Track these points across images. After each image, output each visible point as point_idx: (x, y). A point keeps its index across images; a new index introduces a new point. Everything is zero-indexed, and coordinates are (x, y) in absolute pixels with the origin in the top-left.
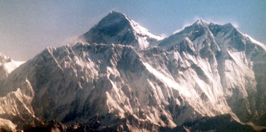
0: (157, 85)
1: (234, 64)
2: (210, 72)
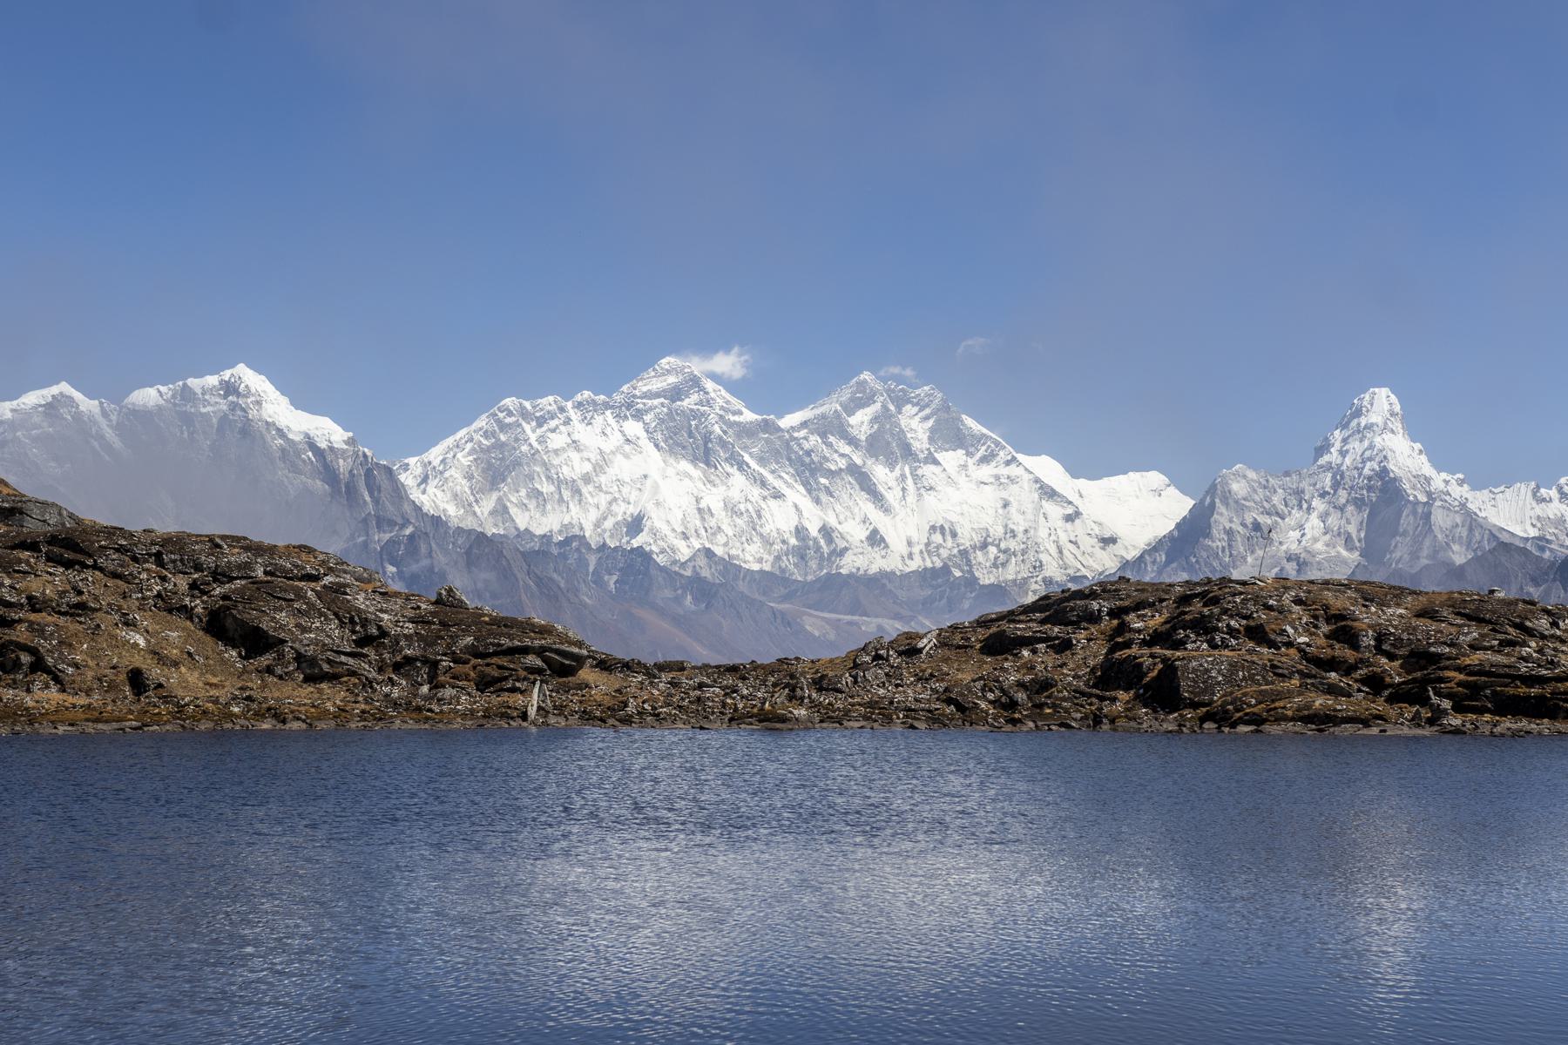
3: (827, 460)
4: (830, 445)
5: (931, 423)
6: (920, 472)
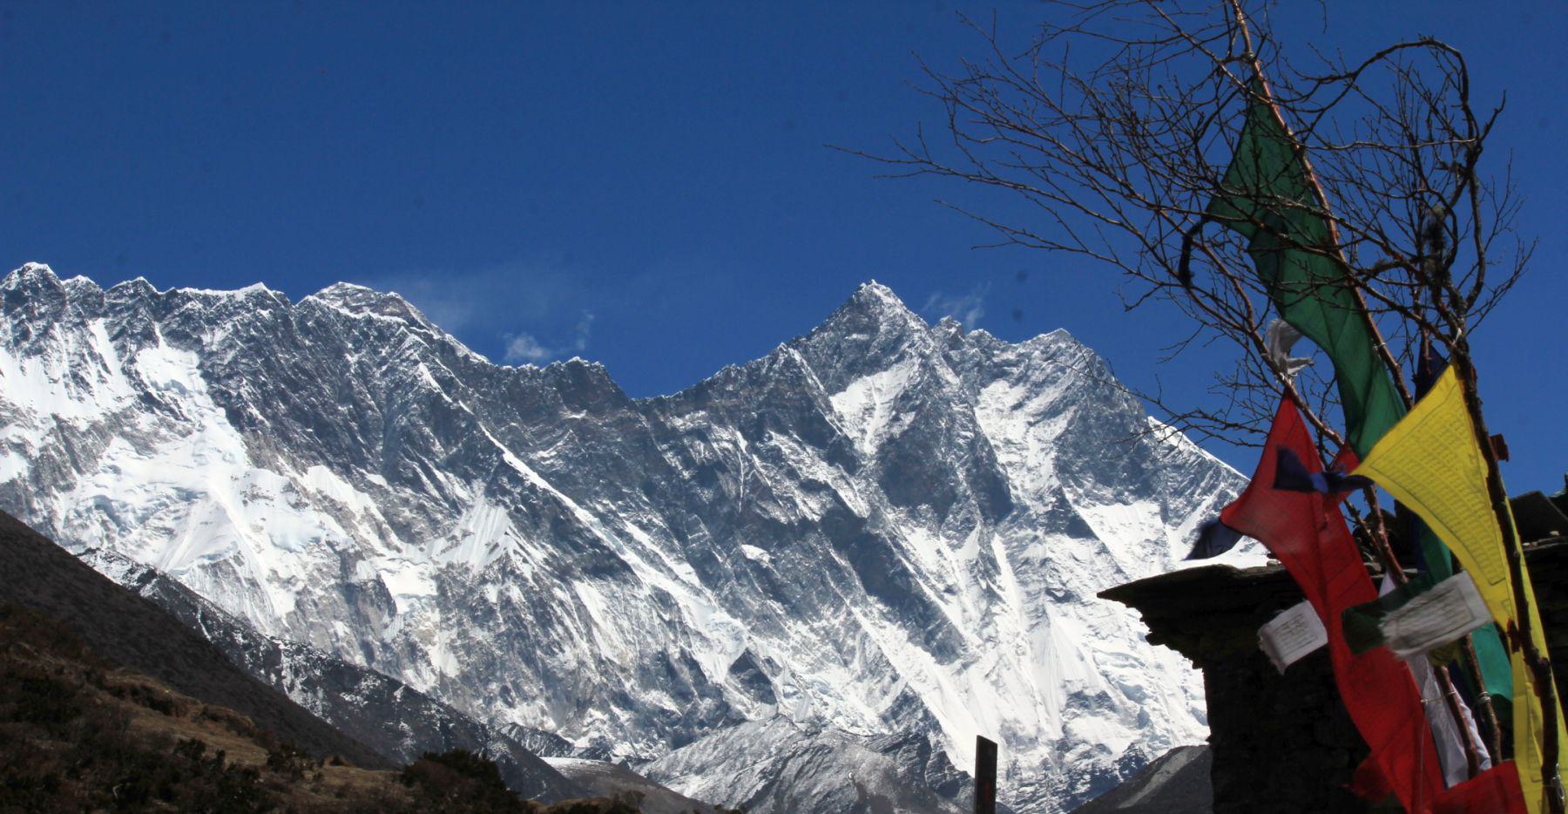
0: (578, 571)
2: (949, 590)
3: (765, 493)
4: (775, 457)
5: (1060, 425)
6: (1035, 552)
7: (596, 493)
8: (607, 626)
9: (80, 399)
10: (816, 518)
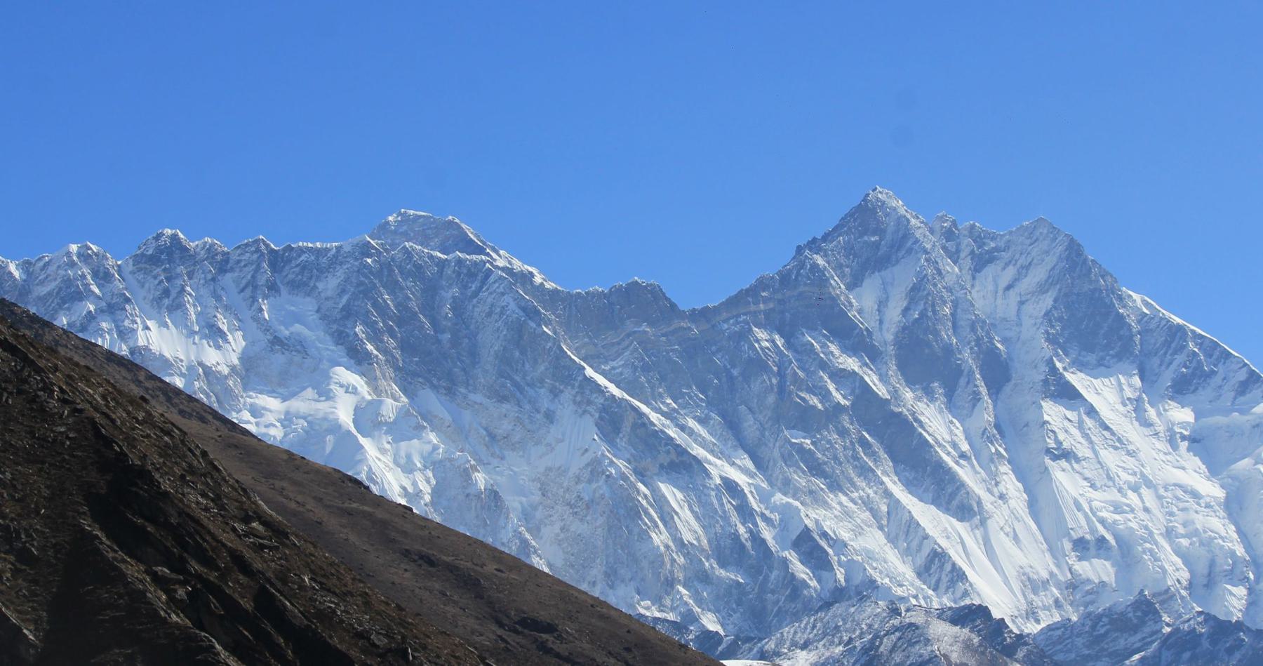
1: (1089, 422)
7: (661, 395)
8: (686, 514)
9: (218, 347)
10: (848, 403)
